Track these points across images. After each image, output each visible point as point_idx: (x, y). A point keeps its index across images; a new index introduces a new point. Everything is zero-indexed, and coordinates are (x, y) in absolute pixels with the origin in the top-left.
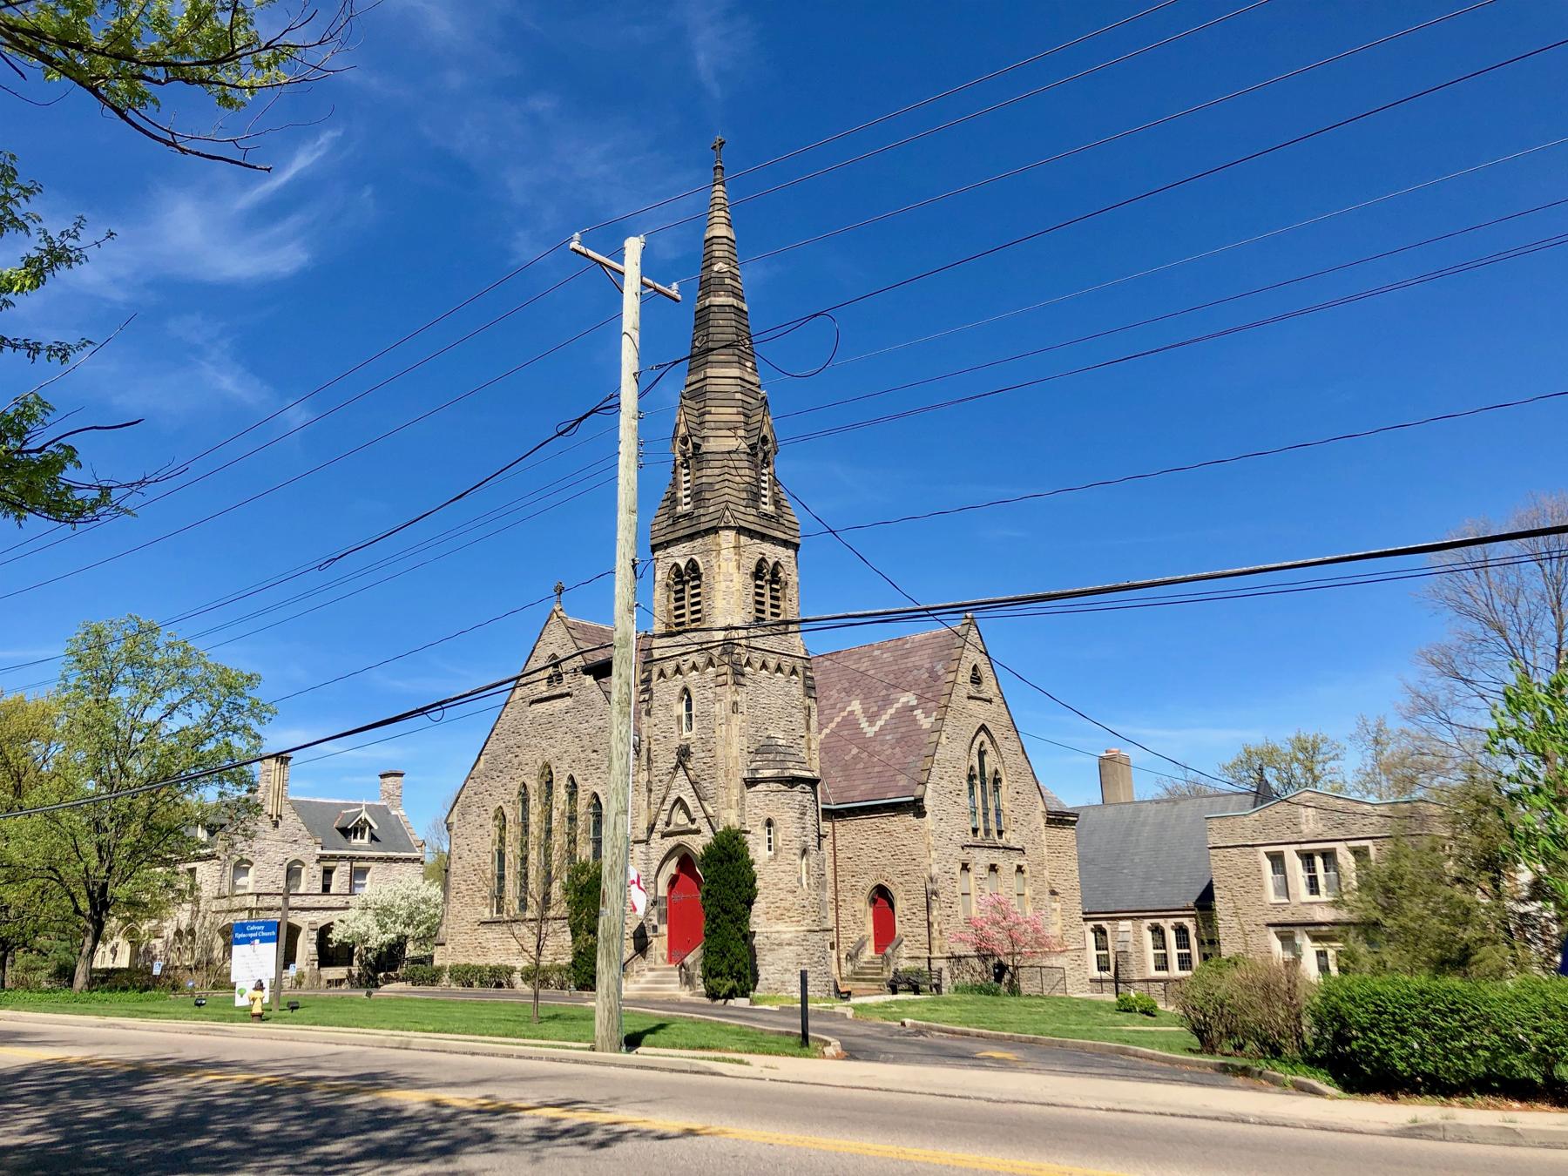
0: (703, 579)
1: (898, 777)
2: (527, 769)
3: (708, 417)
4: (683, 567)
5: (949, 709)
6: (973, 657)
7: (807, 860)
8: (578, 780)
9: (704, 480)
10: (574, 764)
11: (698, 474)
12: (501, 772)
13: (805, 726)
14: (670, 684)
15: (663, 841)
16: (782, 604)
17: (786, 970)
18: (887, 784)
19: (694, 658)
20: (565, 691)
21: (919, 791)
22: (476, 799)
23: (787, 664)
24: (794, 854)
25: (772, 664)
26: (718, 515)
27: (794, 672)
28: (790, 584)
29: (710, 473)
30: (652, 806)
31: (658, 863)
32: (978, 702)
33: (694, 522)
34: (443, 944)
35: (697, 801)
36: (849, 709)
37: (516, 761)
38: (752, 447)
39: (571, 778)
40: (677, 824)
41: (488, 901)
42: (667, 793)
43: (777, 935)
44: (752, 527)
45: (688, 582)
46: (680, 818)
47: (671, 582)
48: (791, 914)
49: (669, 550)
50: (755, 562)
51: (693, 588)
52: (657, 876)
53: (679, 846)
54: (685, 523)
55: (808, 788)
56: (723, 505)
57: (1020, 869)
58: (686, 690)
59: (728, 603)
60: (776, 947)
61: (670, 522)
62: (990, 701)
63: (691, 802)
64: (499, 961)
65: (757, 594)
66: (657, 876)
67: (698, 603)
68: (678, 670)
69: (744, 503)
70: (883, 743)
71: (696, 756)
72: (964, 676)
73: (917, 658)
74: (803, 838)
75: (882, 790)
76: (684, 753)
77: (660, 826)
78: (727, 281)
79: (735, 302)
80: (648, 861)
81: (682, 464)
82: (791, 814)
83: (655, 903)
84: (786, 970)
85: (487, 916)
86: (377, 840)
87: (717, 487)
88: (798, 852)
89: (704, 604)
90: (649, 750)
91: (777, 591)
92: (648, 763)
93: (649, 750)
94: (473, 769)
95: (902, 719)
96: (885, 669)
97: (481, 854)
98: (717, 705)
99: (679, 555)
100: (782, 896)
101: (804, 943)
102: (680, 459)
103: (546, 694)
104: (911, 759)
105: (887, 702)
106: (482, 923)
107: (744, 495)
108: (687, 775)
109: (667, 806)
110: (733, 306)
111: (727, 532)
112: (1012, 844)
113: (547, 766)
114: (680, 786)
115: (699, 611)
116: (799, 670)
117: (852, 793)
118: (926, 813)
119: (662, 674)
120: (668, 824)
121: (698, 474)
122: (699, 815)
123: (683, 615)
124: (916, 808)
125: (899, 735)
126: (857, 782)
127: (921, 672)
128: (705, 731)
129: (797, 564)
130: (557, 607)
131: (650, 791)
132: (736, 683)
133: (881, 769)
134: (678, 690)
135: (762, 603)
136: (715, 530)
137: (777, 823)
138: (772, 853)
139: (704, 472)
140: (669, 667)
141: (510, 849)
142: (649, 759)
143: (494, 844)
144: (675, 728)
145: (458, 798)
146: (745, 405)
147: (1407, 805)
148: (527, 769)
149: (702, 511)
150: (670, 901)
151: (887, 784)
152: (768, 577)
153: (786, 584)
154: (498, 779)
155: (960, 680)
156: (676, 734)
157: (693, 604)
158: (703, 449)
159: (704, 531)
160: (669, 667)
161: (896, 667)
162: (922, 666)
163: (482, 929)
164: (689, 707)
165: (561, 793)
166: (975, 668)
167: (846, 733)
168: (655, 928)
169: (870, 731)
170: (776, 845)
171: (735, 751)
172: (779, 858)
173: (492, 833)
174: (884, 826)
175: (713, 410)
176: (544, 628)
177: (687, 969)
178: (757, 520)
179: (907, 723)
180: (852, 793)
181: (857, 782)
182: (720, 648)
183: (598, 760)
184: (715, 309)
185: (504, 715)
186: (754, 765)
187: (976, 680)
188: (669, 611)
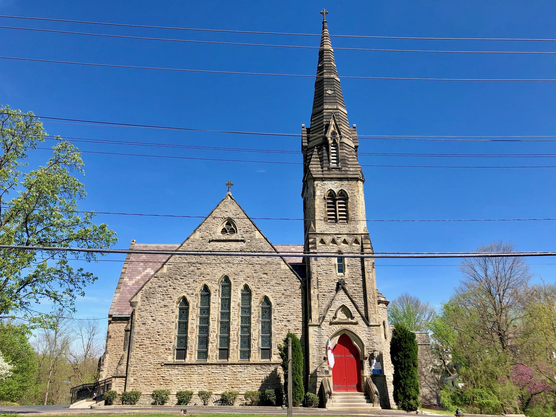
0: (350, 200)
2: (208, 277)
8: (252, 287)
10: (248, 279)
12: (184, 276)
14: (328, 247)
15: (331, 327)
19: (345, 237)
20: (240, 239)
22: (160, 289)
30: (320, 308)
33: (343, 173)
39: (246, 287)
41: (172, 352)
46: (341, 316)
64: (181, 388)
87: (350, 160)
92: (318, 285)
97: (165, 323)
99: (335, 186)
106: (165, 364)
113: (227, 278)
114: (342, 299)
120: (334, 318)
136: (357, 179)
141: (193, 322)
144: (333, 270)
145: (143, 287)
147: (425, 334)
148: (208, 277)
149: (347, 169)
154: (182, 280)
156: (334, 272)
163: (165, 368)
176: (220, 203)
183: (267, 279)
184: (335, 81)
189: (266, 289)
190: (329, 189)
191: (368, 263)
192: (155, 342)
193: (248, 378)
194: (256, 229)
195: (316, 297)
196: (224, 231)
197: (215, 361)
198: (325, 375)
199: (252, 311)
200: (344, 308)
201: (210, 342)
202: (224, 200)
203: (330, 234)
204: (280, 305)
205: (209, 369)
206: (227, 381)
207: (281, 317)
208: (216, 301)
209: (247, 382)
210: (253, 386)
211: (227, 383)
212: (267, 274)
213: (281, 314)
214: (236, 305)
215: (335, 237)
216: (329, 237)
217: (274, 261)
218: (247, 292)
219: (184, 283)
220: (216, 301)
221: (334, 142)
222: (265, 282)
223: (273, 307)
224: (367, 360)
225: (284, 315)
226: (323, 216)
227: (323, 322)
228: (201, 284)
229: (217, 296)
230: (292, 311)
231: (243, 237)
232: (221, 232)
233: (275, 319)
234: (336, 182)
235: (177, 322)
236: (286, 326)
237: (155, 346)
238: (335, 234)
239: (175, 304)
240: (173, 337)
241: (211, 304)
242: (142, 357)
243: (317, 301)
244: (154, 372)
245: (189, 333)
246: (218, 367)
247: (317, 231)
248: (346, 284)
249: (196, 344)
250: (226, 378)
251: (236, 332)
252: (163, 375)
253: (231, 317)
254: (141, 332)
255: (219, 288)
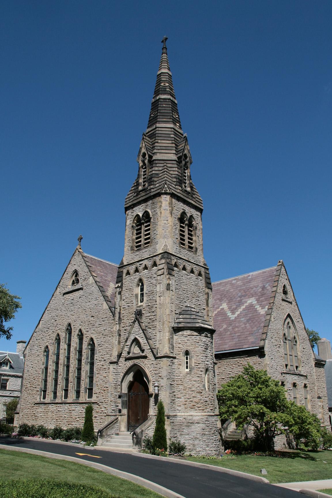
0: (152, 220)
1: (249, 338)
3: (156, 144)
4: (141, 215)
5: (274, 304)
6: (283, 281)
7: (208, 375)
8: (84, 331)
9: (154, 172)
11: (150, 170)
13: (205, 303)
14: (132, 277)
15: (126, 363)
16: (194, 238)
17: (196, 438)
18: (243, 341)
20: (80, 287)
21: (262, 343)
23: (196, 269)
24: (201, 371)
25: (189, 268)
26: (161, 187)
27: (200, 274)
28: (198, 228)
29: (156, 169)
31: (123, 375)
32: (286, 303)
33: (148, 192)
34: (18, 413)
35: (145, 340)
36: (221, 307)
37: (55, 323)
38: (179, 158)
39: (80, 331)
40: (134, 353)
42: (129, 336)
43: (191, 417)
44: (179, 195)
45: (143, 223)
46: (136, 350)
47: (134, 225)
48: (199, 405)
49: (134, 209)
50: (180, 213)
51: (146, 227)
52: (122, 382)
53: (135, 365)
54: (143, 194)
55: (209, 335)
56: (163, 182)
57: (305, 386)
58: (141, 280)
59: (165, 232)
60: (190, 424)
61: (135, 195)
62: (291, 303)
63: (143, 341)
64: (42, 424)
65: (181, 230)
66: (122, 382)
67: (149, 234)
68: (137, 270)
69: (175, 183)
70: (240, 322)
71: (146, 315)
72: (280, 290)
73: (255, 282)
74: (206, 362)
75: (241, 344)
76: (139, 314)
77: (124, 354)
78: (167, 90)
79: (171, 98)
80: (117, 374)
81: (142, 166)
82: (200, 348)
83: (120, 397)
84: (196, 438)
85: (38, 400)
86: (13, 368)
87: (160, 175)
88: (204, 370)
89: (152, 233)
90: (120, 313)
91: (191, 231)
93: (120, 313)
94: (36, 327)
95: (250, 310)
96: (239, 289)
98: (158, 286)
99: (139, 211)
100: (194, 395)
101: (207, 422)
102: (141, 164)
103: (71, 289)
104: (255, 329)
105: (241, 303)
106: (36, 403)
107: (175, 180)
108: (140, 326)
109: (129, 343)
110: (170, 99)
111: (165, 196)
112: (302, 373)
113: (69, 325)
115: (149, 238)
116: (203, 273)
117: (225, 346)
118: (265, 355)
119: (128, 273)
120: (129, 353)
121: (150, 170)
122: (146, 347)
123: (140, 241)
124: (260, 353)
125: (248, 318)
126: (226, 341)
127: (258, 288)
128: (150, 301)
129: (201, 219)
130: (78, 247)
131: (120, 335)
132: (169, 274)
133: (239, 334)
134: (136, 280)
135: (184, 232)
136: (159, 195)
137: (192, 353)
138: (188, 370)
139: (154, 169)
140: (132, 269)
142: (119, 318)
143: (43, 364)
144: (134, 301)
146: (176, 140)
149: (152, 187)
150: (129, 396)
151: (243, 341)
152: (187, 222)
153: (196, 228)
155: (278, 291)
156: (134, 304)
157: (146, 235)
158: (154, 158)
159: (153, 196)
160: (132, 269)
161: (244, 287)
162: (258, 286)
164: (142, 290)
165: (75, 340)
166: (284, 286)
167: (220, 318)
168: (120, 411)
169: (232, 317)
170: (191, 365)
171: (168, 312)
172: (193, 373)
173: (43, 359)
174: (241, 362)
175: (159, 141)
177: (137, 436)
178: (181, 192)
179: (252, 312)
180: (225, 346)
181: (226, 341)
182: (160, 256)
183: (93, 321)
185: (51, 301)
186: (178, 321)
187: (285, 292)
188: (133, 240)
189: (93, 332)
190: (136, 214)
191: (160, 286)
192: (32, 385)
193: (77, 416)
194: (91, 275)
195: (117, 333)
196: (73, 283)
197: (60, 401)
198: (118, 414)
199: (83, 353)
200: (136, 341)
201: (58, 384)
202: (74, 255)
203: (134, 263)
204: (100, 345)
205: (57, 408)
206: (66, 418)
207: (100, 357)
208: (64, 346)
209: (77, 419)
210: (80, 423)
211: (66, 421)
212: (93, 316)
213: (101, 354)
214: (74, 349)
215: (138, 264)
216: (134, 266)
217: (99, 303)
218: (81, 336)
219: (48, 335)
220: (64, 346)
221: (144, 164)
222: (92, 325)
223: (96, 348)
224: (152, 398)
225: (102, 355)
226: (130, 245)
227: (121, 359)
228: (56, 334)
229: (64, 343)
230: (107, 350)
231: (82, 285)
232: (72, 284)
233: (96, 359)
234: (142, 205)
235: (43, 368)
236: (102, 365)
237: (32, 388)
238: (138, 262)
239: (43, 352)
240: (40, 380)
241: (60, 350)
242: (26, 398)
243: (118, 337)
244: (31, 410)
245: (48, 377)
246: (61, 406)
247: (125, 263)
248: (143, 314)
249: (52, 385)
250: (65, 415)
251: (72, 374)
252: (34, 412)
253: (70, 360)
254: (28, 378)
255: (66, 335)
